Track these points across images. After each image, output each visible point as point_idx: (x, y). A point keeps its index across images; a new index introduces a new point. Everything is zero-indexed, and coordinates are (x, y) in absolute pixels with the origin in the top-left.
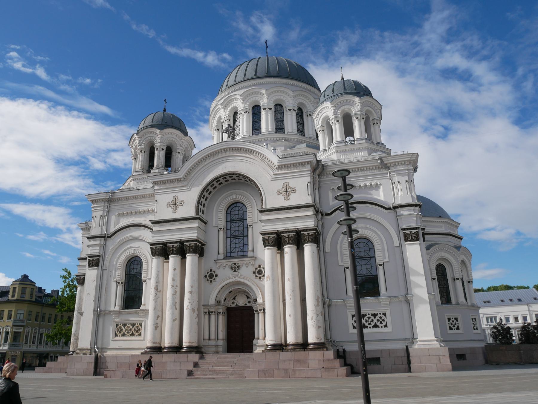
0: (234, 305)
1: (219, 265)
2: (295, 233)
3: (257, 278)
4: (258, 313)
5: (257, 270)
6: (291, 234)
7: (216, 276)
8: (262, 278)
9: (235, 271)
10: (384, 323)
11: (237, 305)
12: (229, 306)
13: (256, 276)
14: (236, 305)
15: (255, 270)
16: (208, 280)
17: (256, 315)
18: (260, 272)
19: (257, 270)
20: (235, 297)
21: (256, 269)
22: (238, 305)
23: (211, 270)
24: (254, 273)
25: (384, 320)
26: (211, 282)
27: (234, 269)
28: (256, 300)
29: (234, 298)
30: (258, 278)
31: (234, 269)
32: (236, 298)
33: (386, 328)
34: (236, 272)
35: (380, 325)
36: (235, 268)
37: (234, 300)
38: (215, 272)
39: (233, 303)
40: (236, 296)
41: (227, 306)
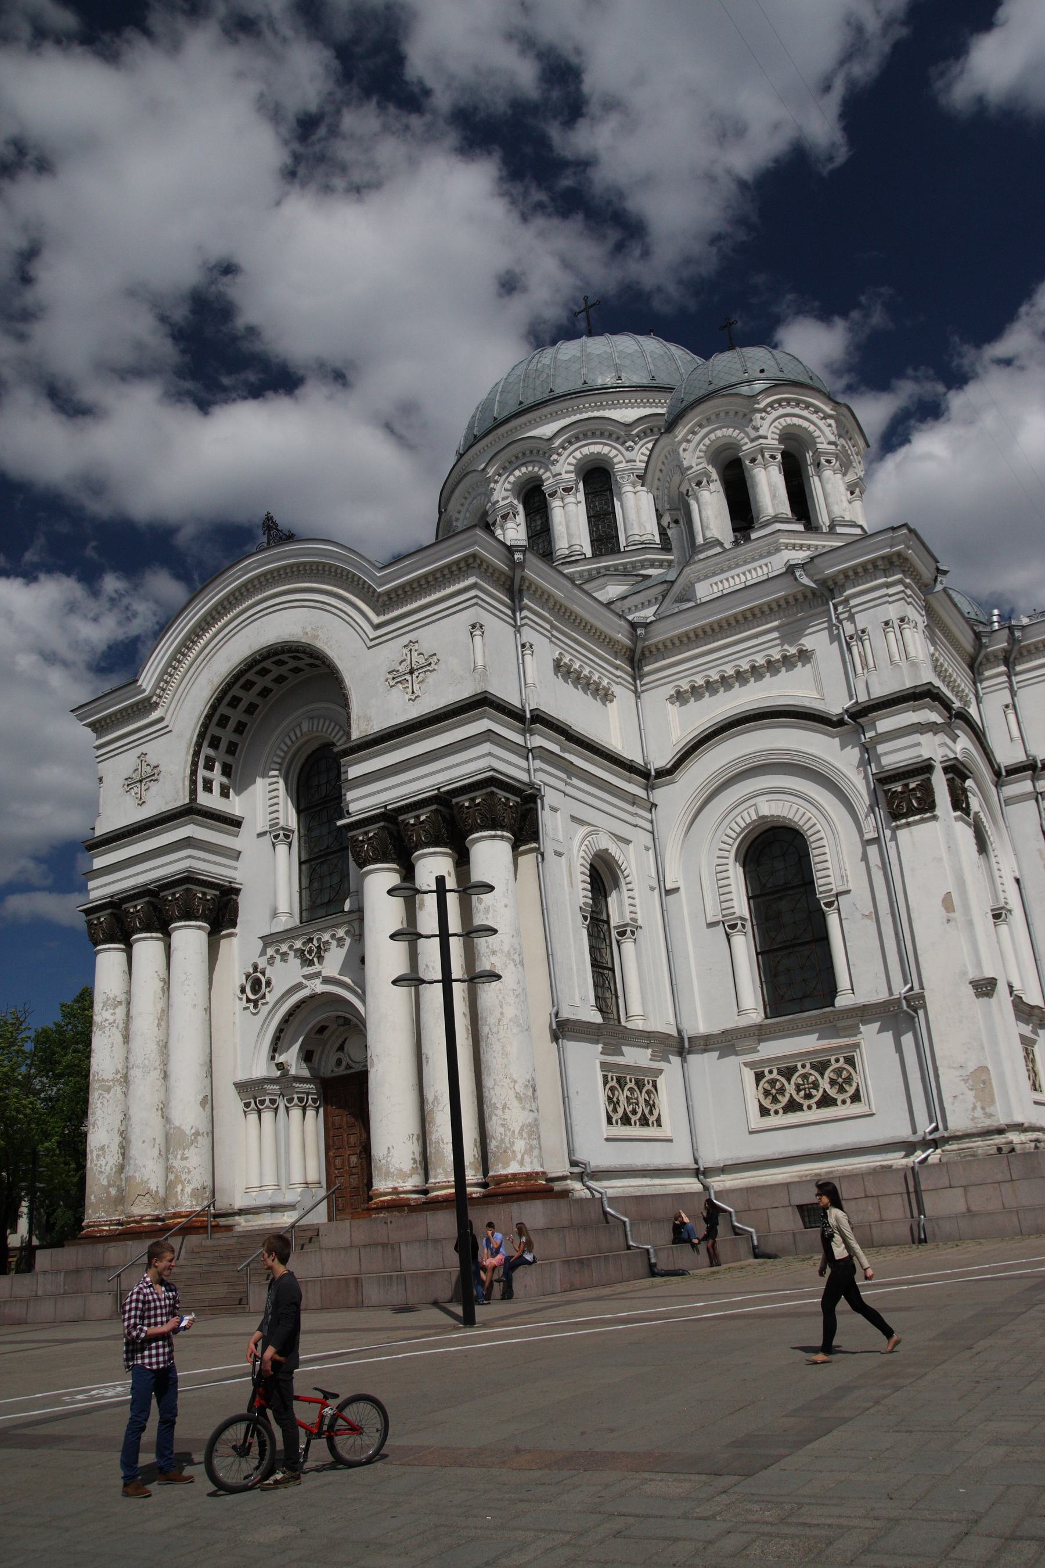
0: (341, 1071)
1: (270, 951)
7: (268, 983)
9: (311, 963)
10: (851, 1090)
11: (349, 1067)
12: (329, 1075)
14: (346, 1068)
16: (248, 1000)
20: (344, 1042)
22: (351, 1068)
23: (255, 968)
25: (849, 1080)
26: (256, 1003)
27: (308, 956)
29: (341, 1048)
31: (308, 956)
32: (346, 1046)
33: (856, 1105)
34: (313, 967)
35: (840, 1098)
36: (310, 952)
37: (340, 1055)
38: (263, 973)
39: (339, 1062)
40: (345, 1040)
41: (322, 1075)
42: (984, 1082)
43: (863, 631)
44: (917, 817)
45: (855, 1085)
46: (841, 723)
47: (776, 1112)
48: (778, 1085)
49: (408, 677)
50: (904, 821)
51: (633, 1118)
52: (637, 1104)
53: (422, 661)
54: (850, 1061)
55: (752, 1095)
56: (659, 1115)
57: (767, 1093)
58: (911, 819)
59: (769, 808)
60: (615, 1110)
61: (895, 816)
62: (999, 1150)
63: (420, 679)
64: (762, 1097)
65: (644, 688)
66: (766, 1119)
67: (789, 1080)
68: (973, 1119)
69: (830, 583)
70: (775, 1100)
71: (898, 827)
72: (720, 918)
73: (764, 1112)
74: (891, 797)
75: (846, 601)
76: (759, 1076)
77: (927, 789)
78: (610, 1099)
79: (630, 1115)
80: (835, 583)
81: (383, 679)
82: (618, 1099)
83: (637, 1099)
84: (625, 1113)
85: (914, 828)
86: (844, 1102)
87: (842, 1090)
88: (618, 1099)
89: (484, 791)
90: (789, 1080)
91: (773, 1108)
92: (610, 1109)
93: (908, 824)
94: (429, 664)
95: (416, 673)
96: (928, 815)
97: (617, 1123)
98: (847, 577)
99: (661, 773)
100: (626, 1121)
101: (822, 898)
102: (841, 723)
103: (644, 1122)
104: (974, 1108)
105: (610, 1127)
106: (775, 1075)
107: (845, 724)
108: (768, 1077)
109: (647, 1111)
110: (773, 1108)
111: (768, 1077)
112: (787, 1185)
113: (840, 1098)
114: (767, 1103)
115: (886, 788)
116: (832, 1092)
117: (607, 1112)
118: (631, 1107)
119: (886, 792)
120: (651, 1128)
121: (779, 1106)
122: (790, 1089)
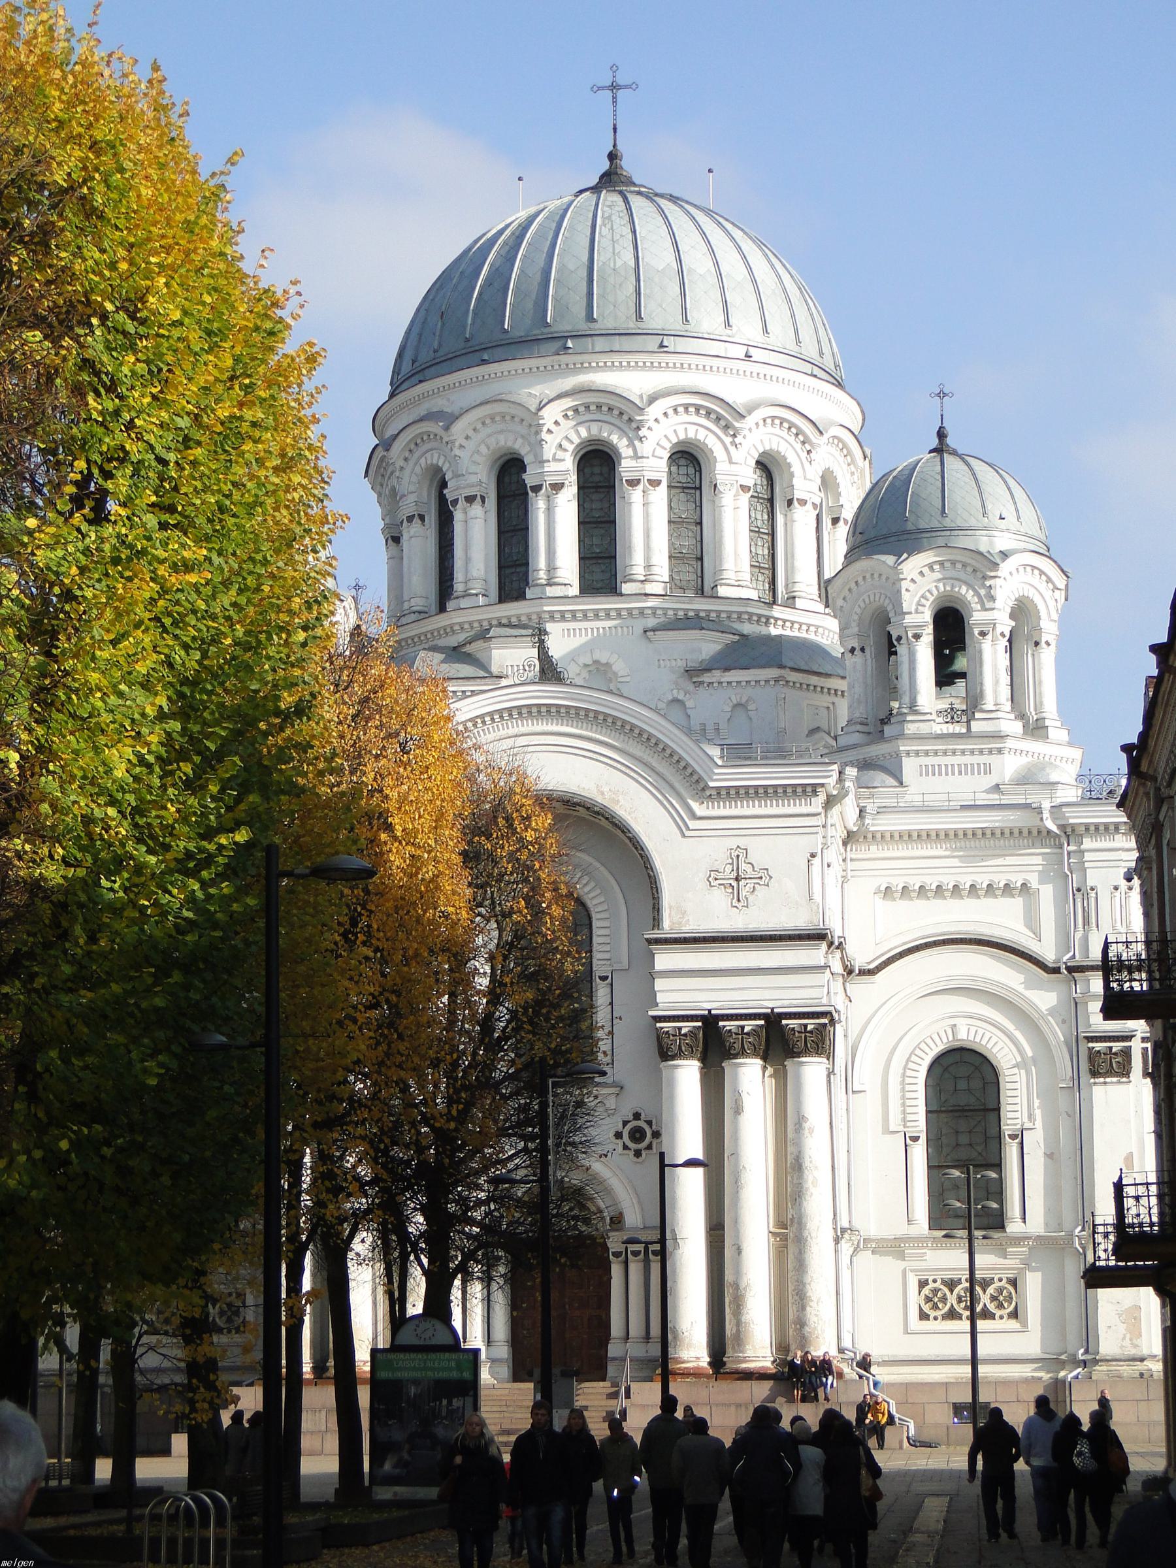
2: (762, 1022)
3: (626, 1152)
4: (626, 1263)
5: (629, 1127)
6: (749, 1026)
8: (644, 1153)
13: (625, 1147)
15: (620, 1125)
17: (616, 1270)
18: (638, 1135)
19: (629, 1127)
21: (625, 1123)
24: (618, 1135)
28: (617, 1221)
30: (632, 1153)
35: (998, 1313)
42: (1135, 1318)
43: (1092, 889)
44: (1115, 1079)
45: (1014, 1304)
46: (1056, 971)
47: (936, 1318)
48: (940, 1294)
49: (734, 884)
50: (1102, 1080)
53: (750, 873)
54: (1014, 1283)
55: (915, 1300)
57: (928, 1299)
58: (1108, 1080)
59: (967, 1034)
61: (1094, 1073)
62: (1142, 1375)
63: (747, 888)
64: (923, 1303)
65: (854, 873)
66: (925, 1322)
67: (952, 1291)
68: (1122, 1347)
69: (1069, 830)
70: (935, 1307)
71: (1095, 1083)
72: (901, 1128)
73: (923, 1316)
74: (1093, 1056)
75: (1082, 852)
76: (922, 1284)
77: (1126, 1053)
80: (1073, 831)
81: (702, 875)
85: (1108, 1087)
86: (1001, 1317)
87: (1000, 1306)
89: (817, 1021)
90: (952, 1291)
91: (932, 1314)
93: (1105, 1083)
94: (763, 877)
95: (742, 883)
96: (1124, 1079)
98: (1087, 829)
99: (862, 972)
101: (1007, 1130)
102: (1056, 971)
104: (1124, 1339)
106: (938, 1285)
107: (1059, 972)
108: (931, 1285)
110: (932, 1314)
111: (931, 1285)
112: (946, 1385)
113: (998, 1313)
114: (926, 1308)
115: (1091, 1045)
116: (991, 1307)
119: (1090, 1049)
121: (939, 1313)
122: (952, 1299)
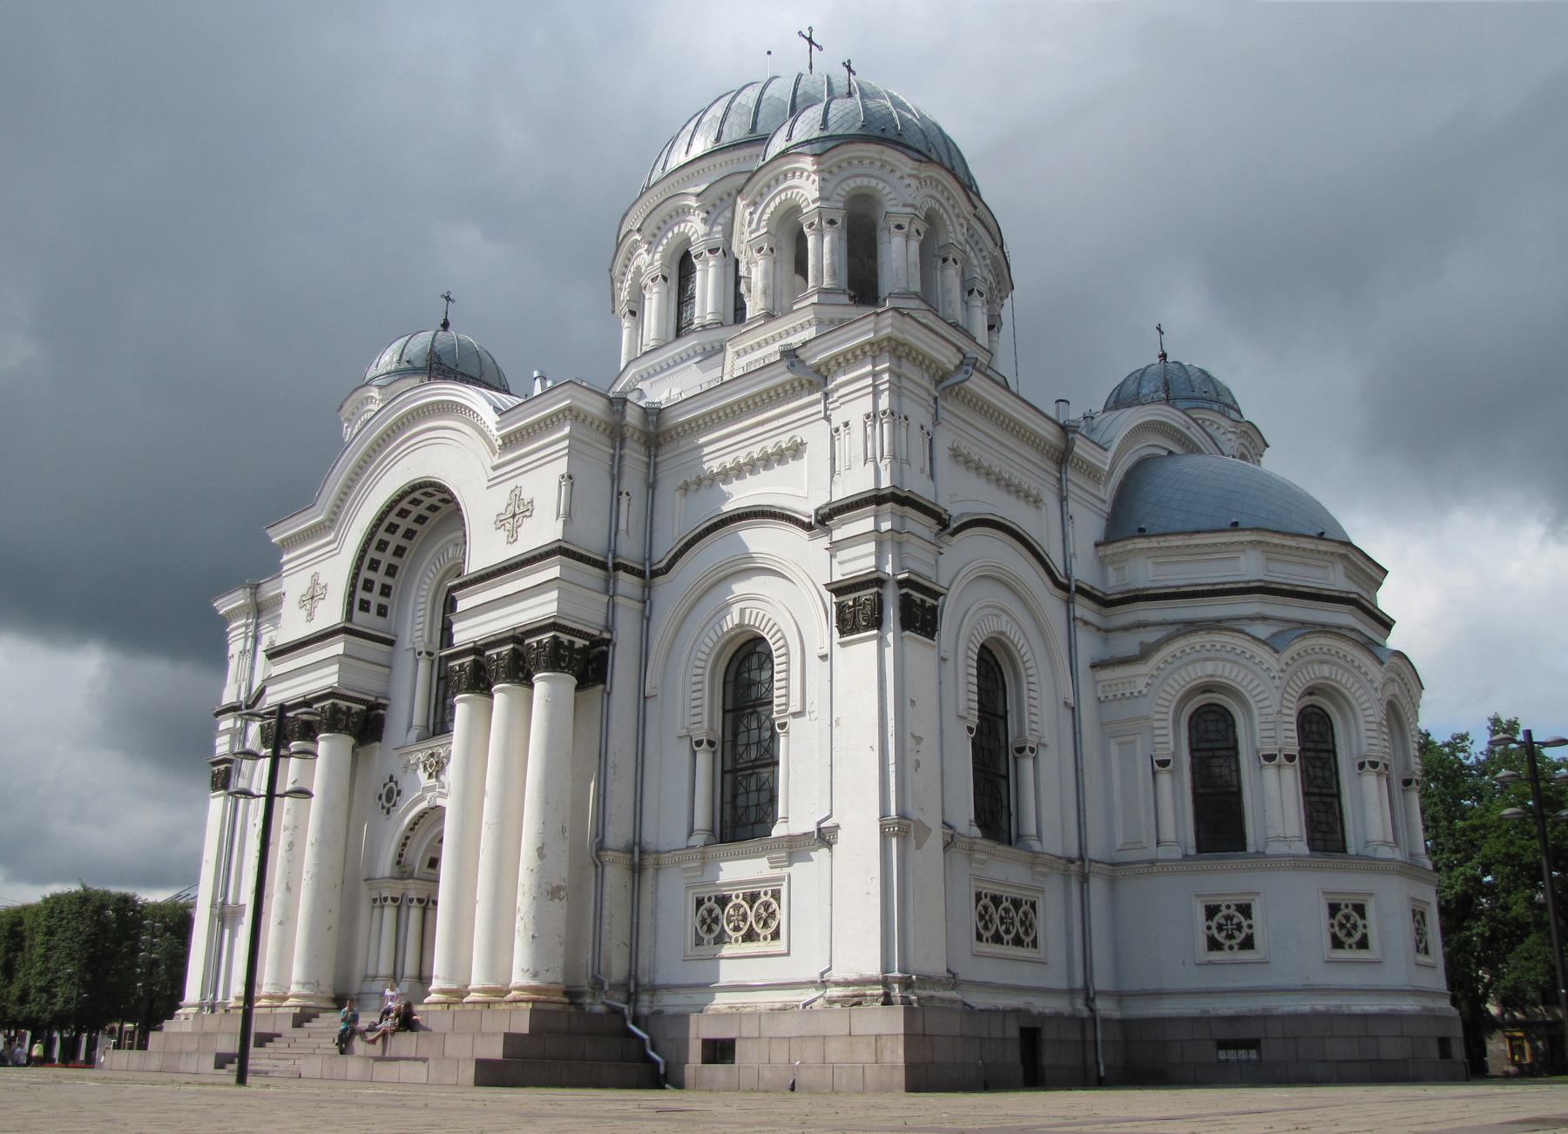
51: (1006, 937)
52: (1013, 924)
56: (1036, 936)
60: (986, 927)
78: (981, 917)
79: (1003, 934)
82: (990, 916)
83: (1012, 918)
84: (997, 931)
88: (990, 916)
92: (981, 925)
97: (987, 941)
100: (997, 939)
103: (1018, 942)
105: (979, 943)
109: (1021, 931)
117: (977, 929)
118: (1004, 927)
120: (1005, 947)
